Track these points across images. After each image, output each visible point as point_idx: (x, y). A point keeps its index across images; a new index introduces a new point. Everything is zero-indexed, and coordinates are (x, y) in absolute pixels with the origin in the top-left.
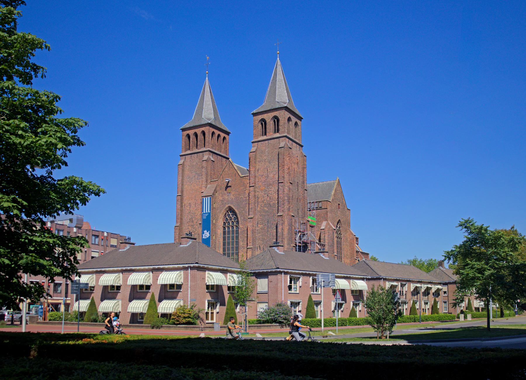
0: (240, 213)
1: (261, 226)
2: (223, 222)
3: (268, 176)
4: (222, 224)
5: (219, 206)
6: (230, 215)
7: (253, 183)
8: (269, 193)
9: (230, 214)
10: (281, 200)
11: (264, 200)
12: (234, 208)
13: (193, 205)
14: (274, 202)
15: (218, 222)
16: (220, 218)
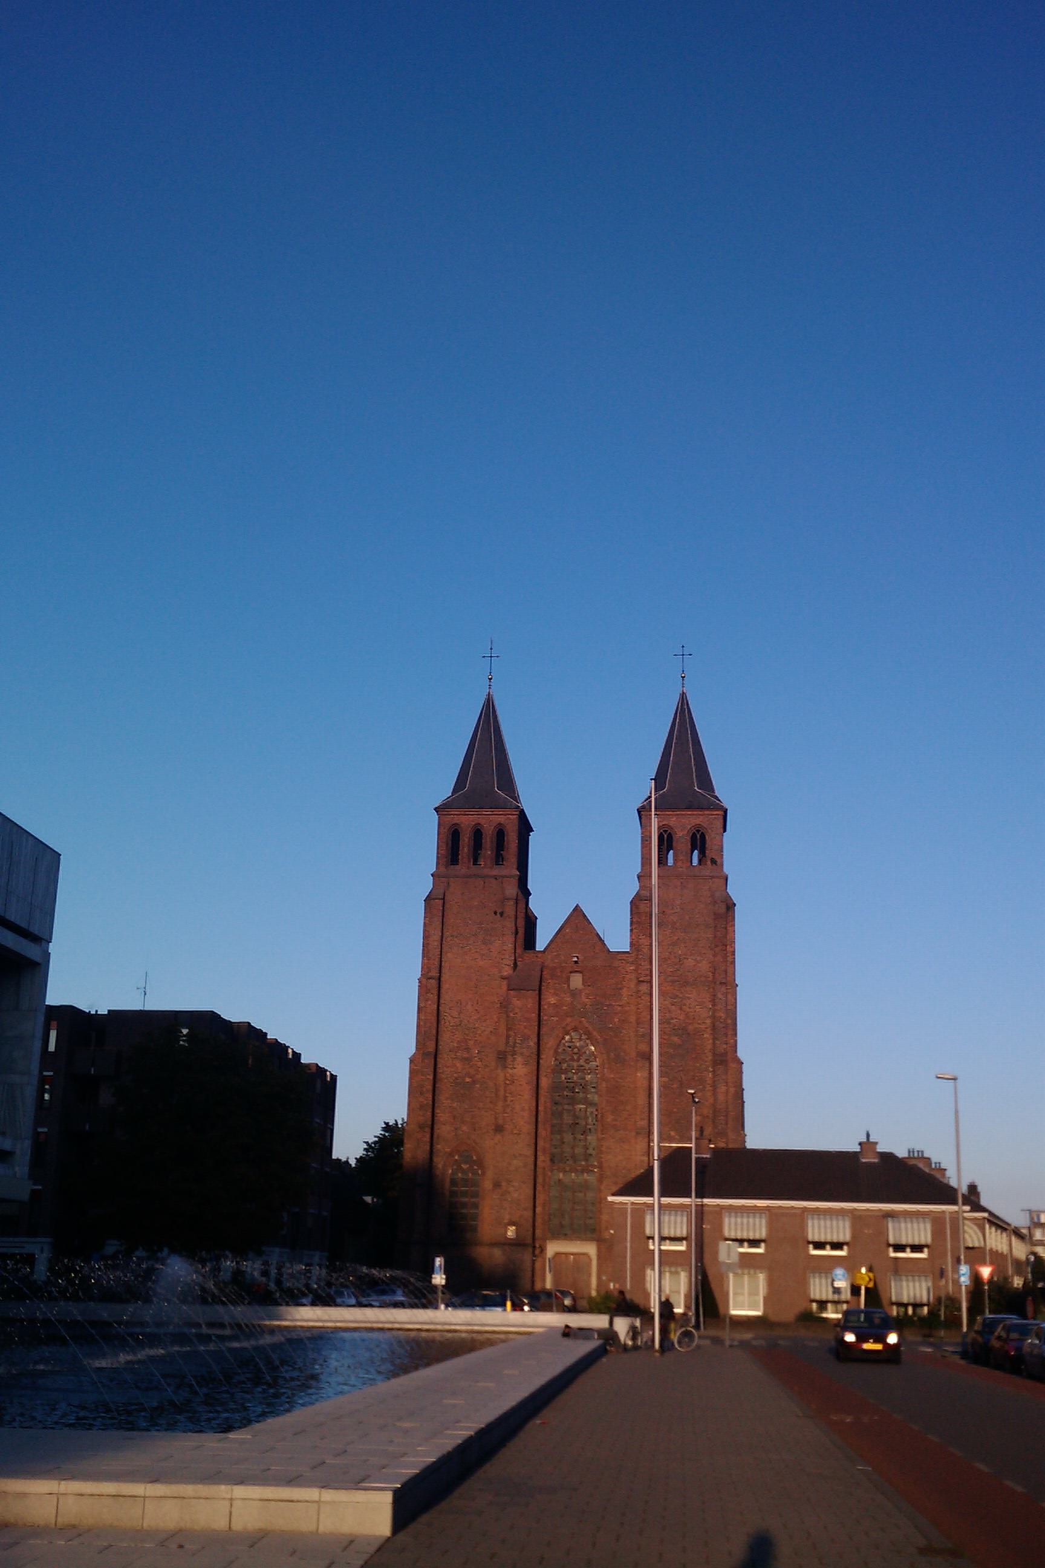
8: (685, 1005)
11: (672, 1019)
13: (469, 1007)
14: (697, 1026)
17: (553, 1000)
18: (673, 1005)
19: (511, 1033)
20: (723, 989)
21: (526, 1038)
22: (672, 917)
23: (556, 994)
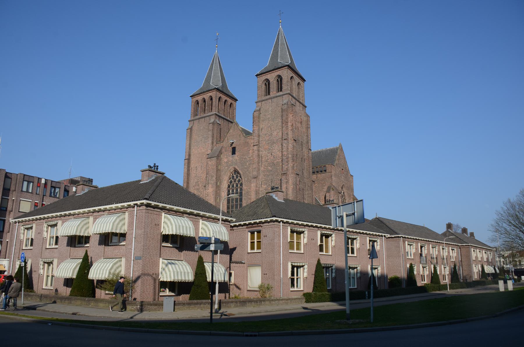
0: (244, 173)
1: (265, 186)
2: (227, 184)
3: (271, 134)
4: (226, 186)
5: (223, 168)
6: (234, 176)
7: (256, 142)
9: (234, 175)
10: (285, 158)
12: (238, 169)
13: (199, 169)
14: (277, 160)
15: (222, 184)
16: (225, 180)
17: (226, 160)
18: (268, 153)
19: (208, 176)
20: (286, 141)
21: (212, 177)
22: (268, 116)
23: (227, 158)
